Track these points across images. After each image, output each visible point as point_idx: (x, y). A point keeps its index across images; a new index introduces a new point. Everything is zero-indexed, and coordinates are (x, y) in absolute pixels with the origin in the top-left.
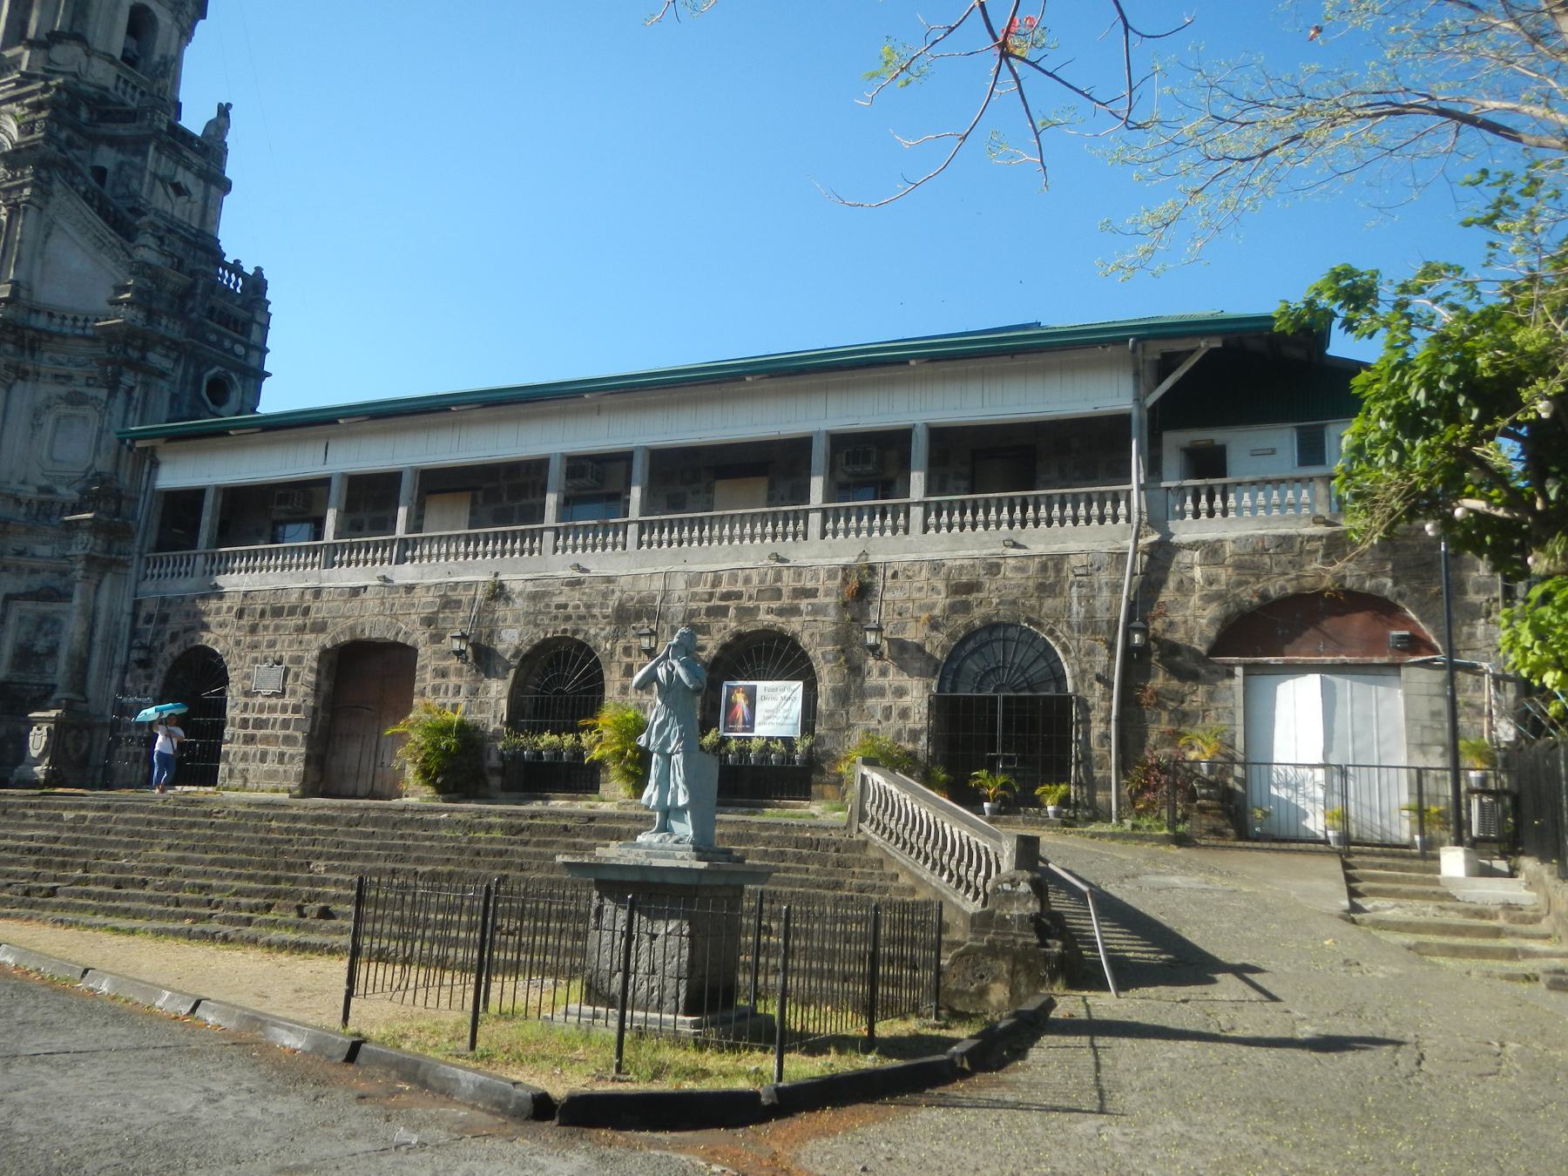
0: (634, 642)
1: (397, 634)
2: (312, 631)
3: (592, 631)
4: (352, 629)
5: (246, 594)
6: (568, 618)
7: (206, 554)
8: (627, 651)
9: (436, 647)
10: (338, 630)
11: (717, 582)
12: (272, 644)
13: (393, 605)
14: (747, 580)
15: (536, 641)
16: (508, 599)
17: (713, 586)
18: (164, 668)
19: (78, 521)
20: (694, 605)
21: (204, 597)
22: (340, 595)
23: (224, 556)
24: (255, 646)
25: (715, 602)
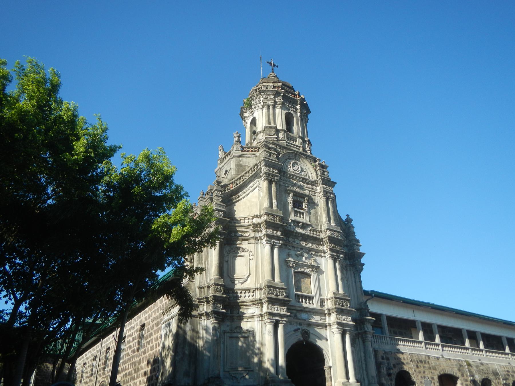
0: (499, 381)
1: (454, 373)
2: (434, 369)
3: (491, 377)
4: (443, 370)
5: (410, 353)
6: (485, 373)
7: (390, 338)
8: (498, 383)
9: (463, 378)
10: (440, 370)
11: (504, 369)
12: (424, 372)
13: (449, 364)
14: (509, 369)
15: (482, 379)
16: (471, 366)
17: (504, 369)
18: (395, 377)
19: (369, 320)
20: (504, 373)
21: (397, 353)
22: (435, 359)
23: (397, 339)
24: (420, 372)
25: (507, 373)
